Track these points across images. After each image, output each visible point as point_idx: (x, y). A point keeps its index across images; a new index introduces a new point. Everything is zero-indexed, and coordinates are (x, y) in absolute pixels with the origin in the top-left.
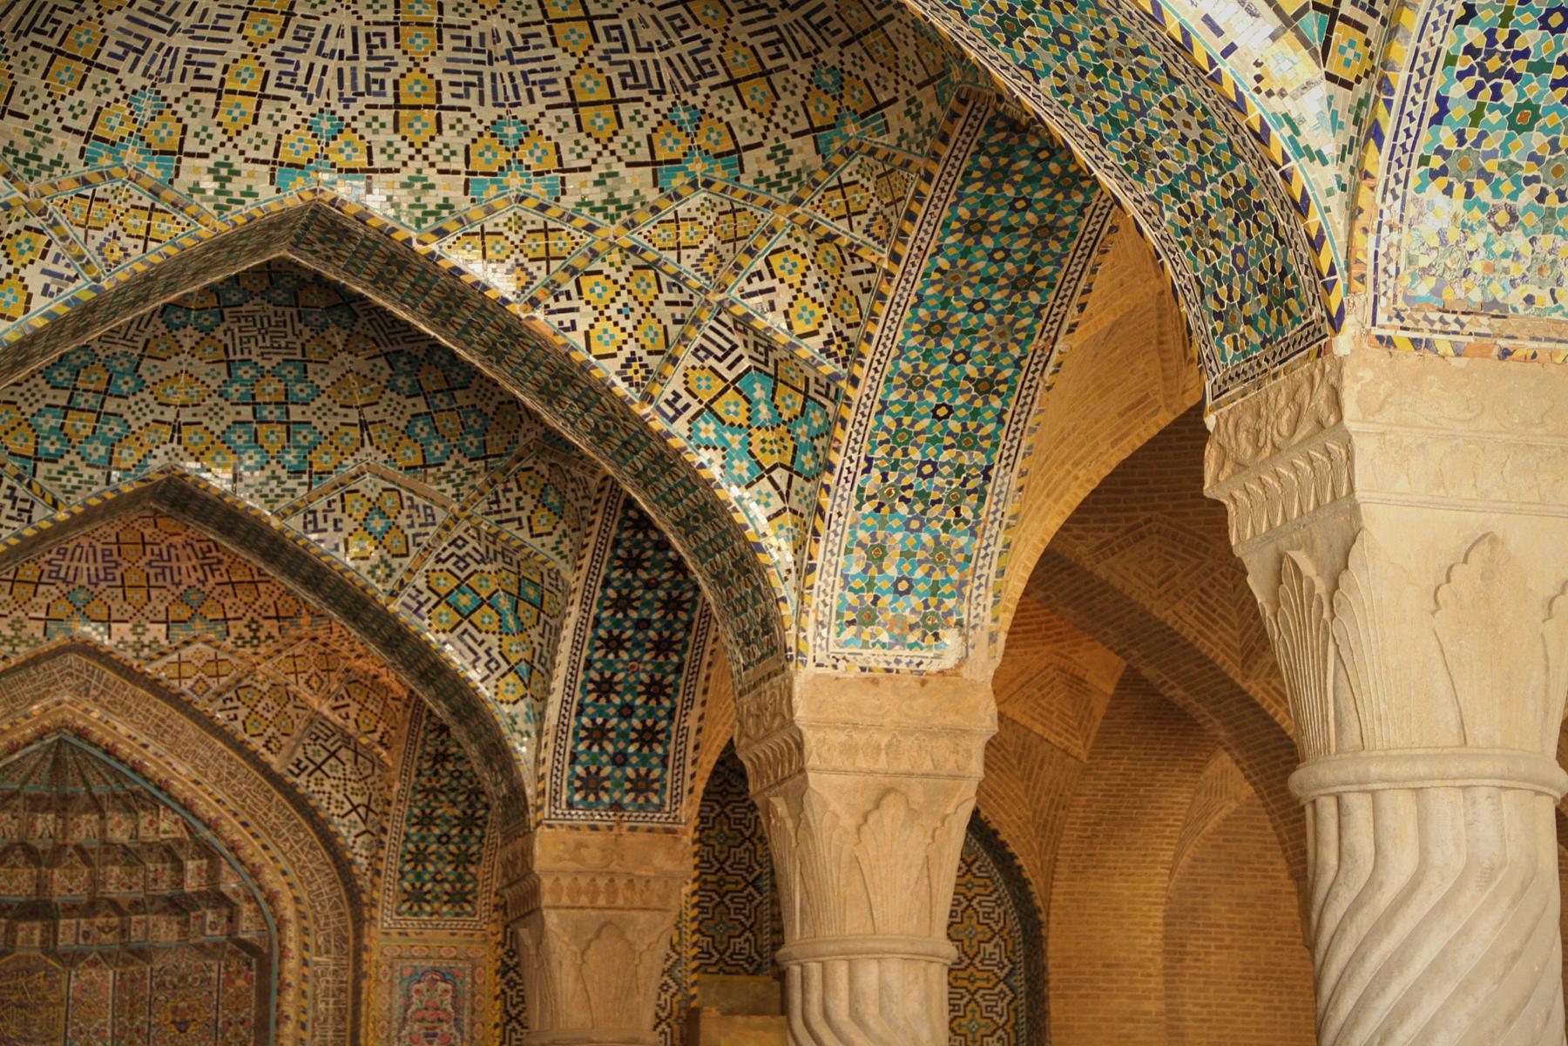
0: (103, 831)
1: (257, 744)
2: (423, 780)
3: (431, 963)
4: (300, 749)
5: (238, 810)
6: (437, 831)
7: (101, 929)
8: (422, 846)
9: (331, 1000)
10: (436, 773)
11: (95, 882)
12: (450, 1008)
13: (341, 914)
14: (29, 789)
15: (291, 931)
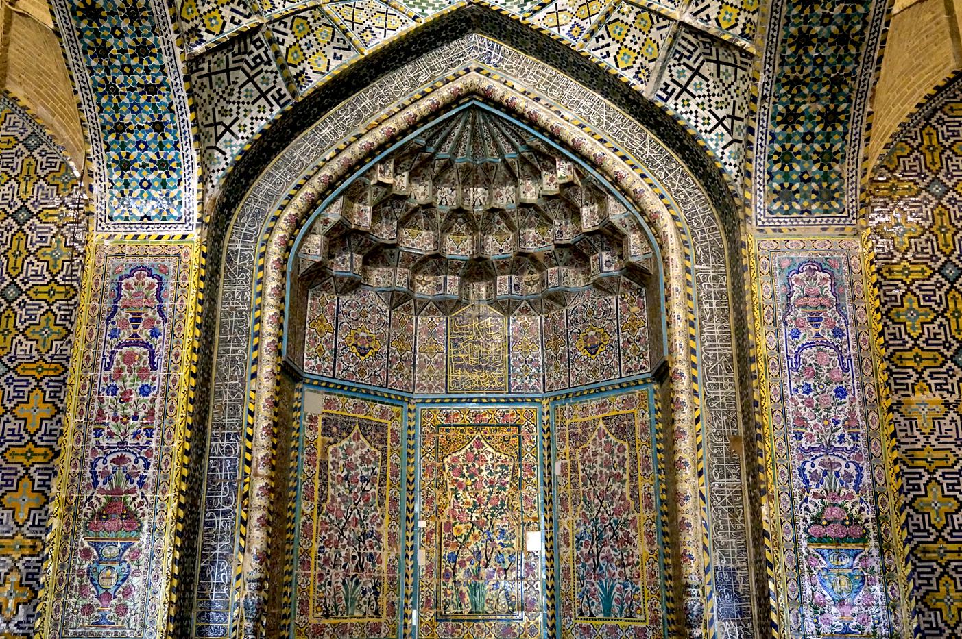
0: (518, 196)
1: (628, 76)
2: (787, 69)
3: (807, 255)
4: (667, 73)
5: (618, 147)
6: (801, 129)
7: (527, 283)
8: (788, 146)
9: (714, 302)
10: (800, 61)
11: (519, 241)
12: (830, 295)
13: (715, 229)
14: (460, 161)
15: (673, 244)
